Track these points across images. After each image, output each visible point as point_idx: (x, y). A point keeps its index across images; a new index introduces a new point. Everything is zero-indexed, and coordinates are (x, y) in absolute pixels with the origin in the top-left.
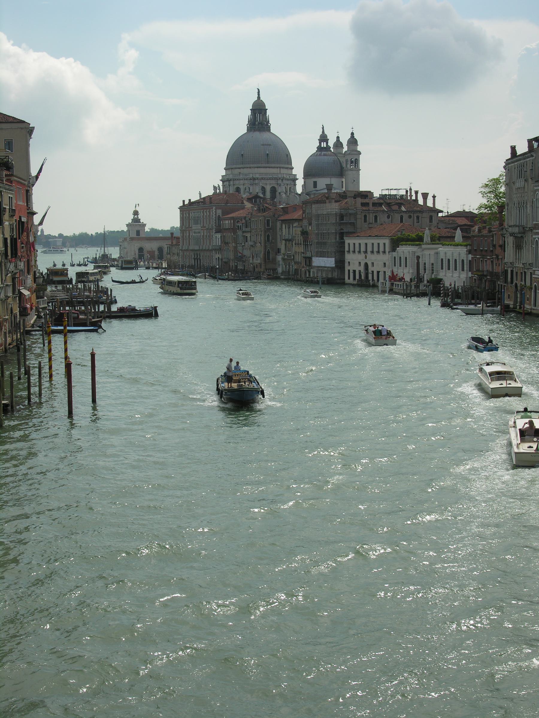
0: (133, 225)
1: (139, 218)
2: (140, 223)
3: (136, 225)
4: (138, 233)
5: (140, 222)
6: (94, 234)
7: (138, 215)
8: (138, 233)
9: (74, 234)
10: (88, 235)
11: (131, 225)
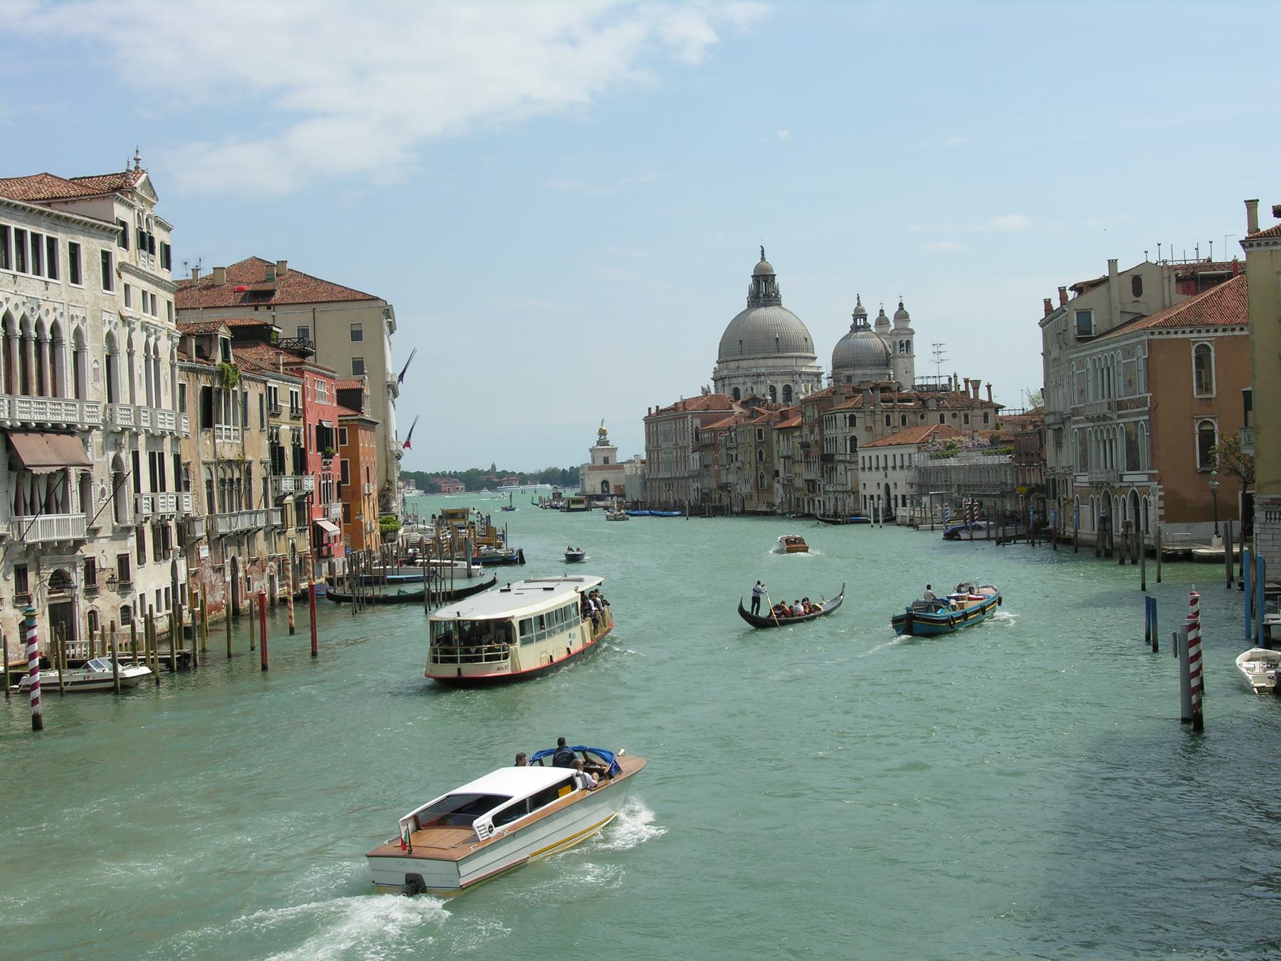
0: (599, 449)
1: (608, 439)
3: (603, 449)
4: (606, 460)
6: (567, 469)
7: (605, 435)
8: (606, 460)
9: (540, 471)
11: (595, 450)
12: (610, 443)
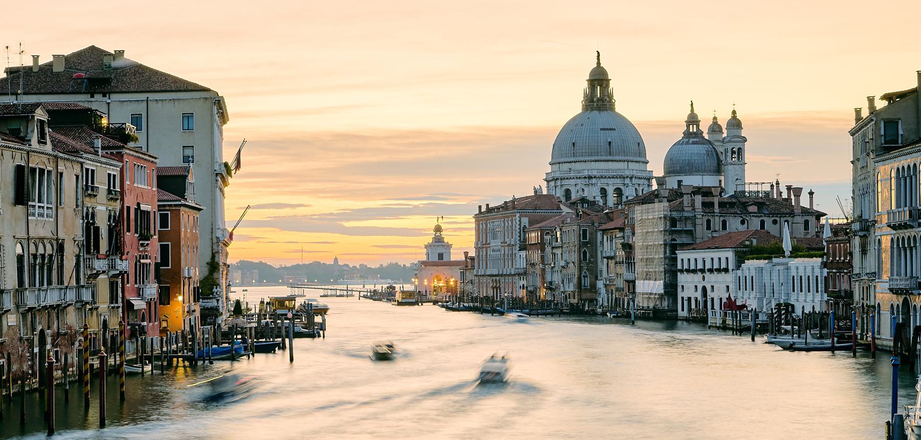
2: (443, 244)
4: (441, 256)
5: (443, 242)
7: (440, 232)
8: (441, 256)
9: (381, 265)
10: (400, 266)
12: (446, 241)
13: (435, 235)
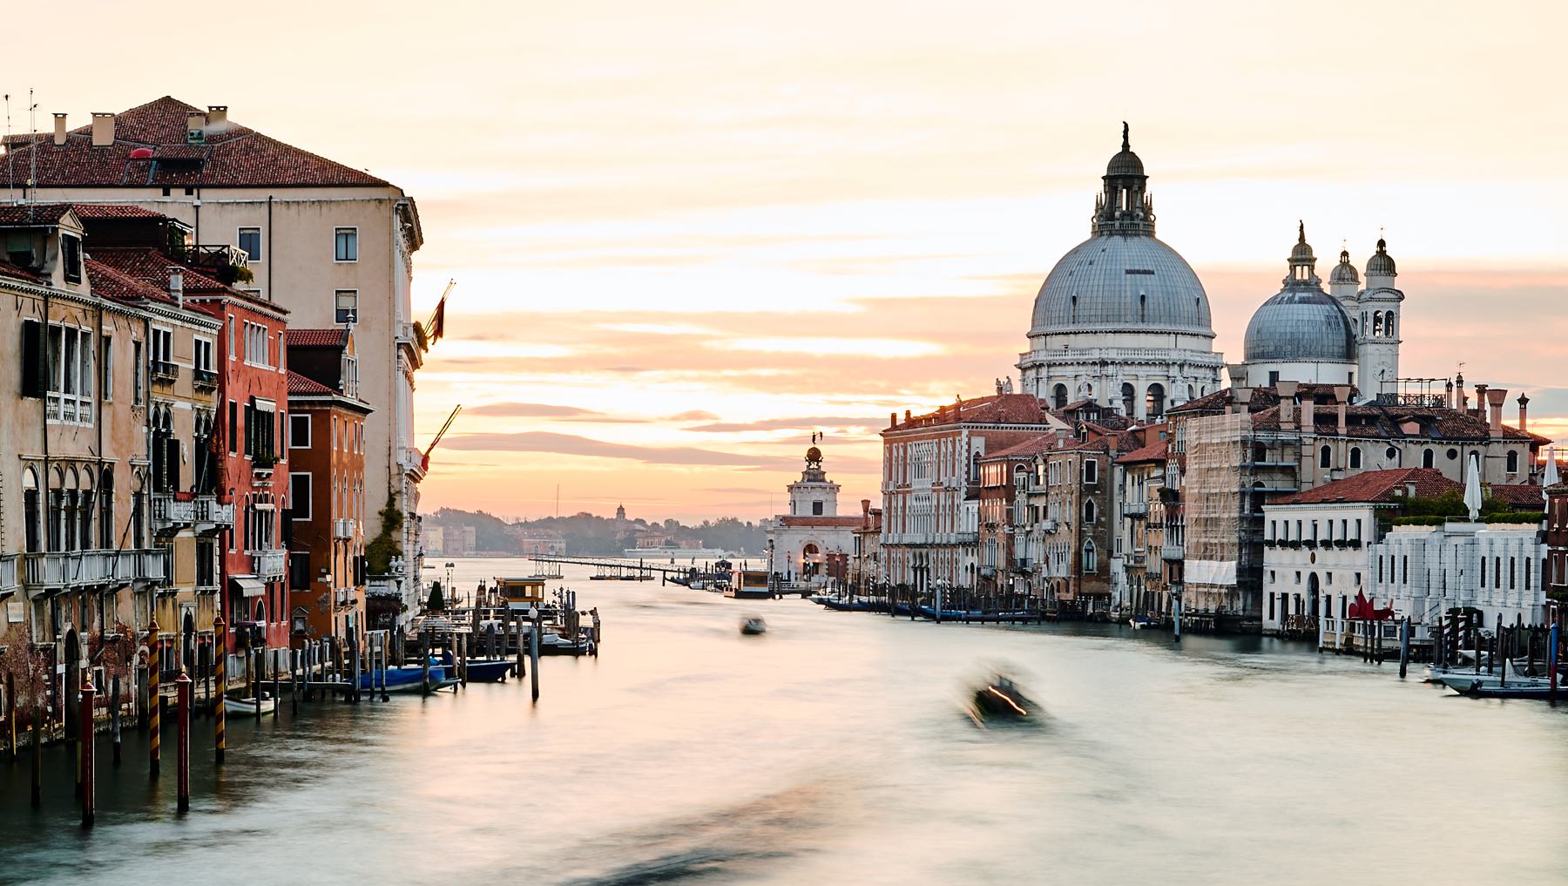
1: (822, 469)
4: (818, 507)
5: (823, 480)
7: (818, 462)
8: (818, 507)
9: (706, 523)
10: (741, 524)
12: (828, 477)
13: (808, 467)
